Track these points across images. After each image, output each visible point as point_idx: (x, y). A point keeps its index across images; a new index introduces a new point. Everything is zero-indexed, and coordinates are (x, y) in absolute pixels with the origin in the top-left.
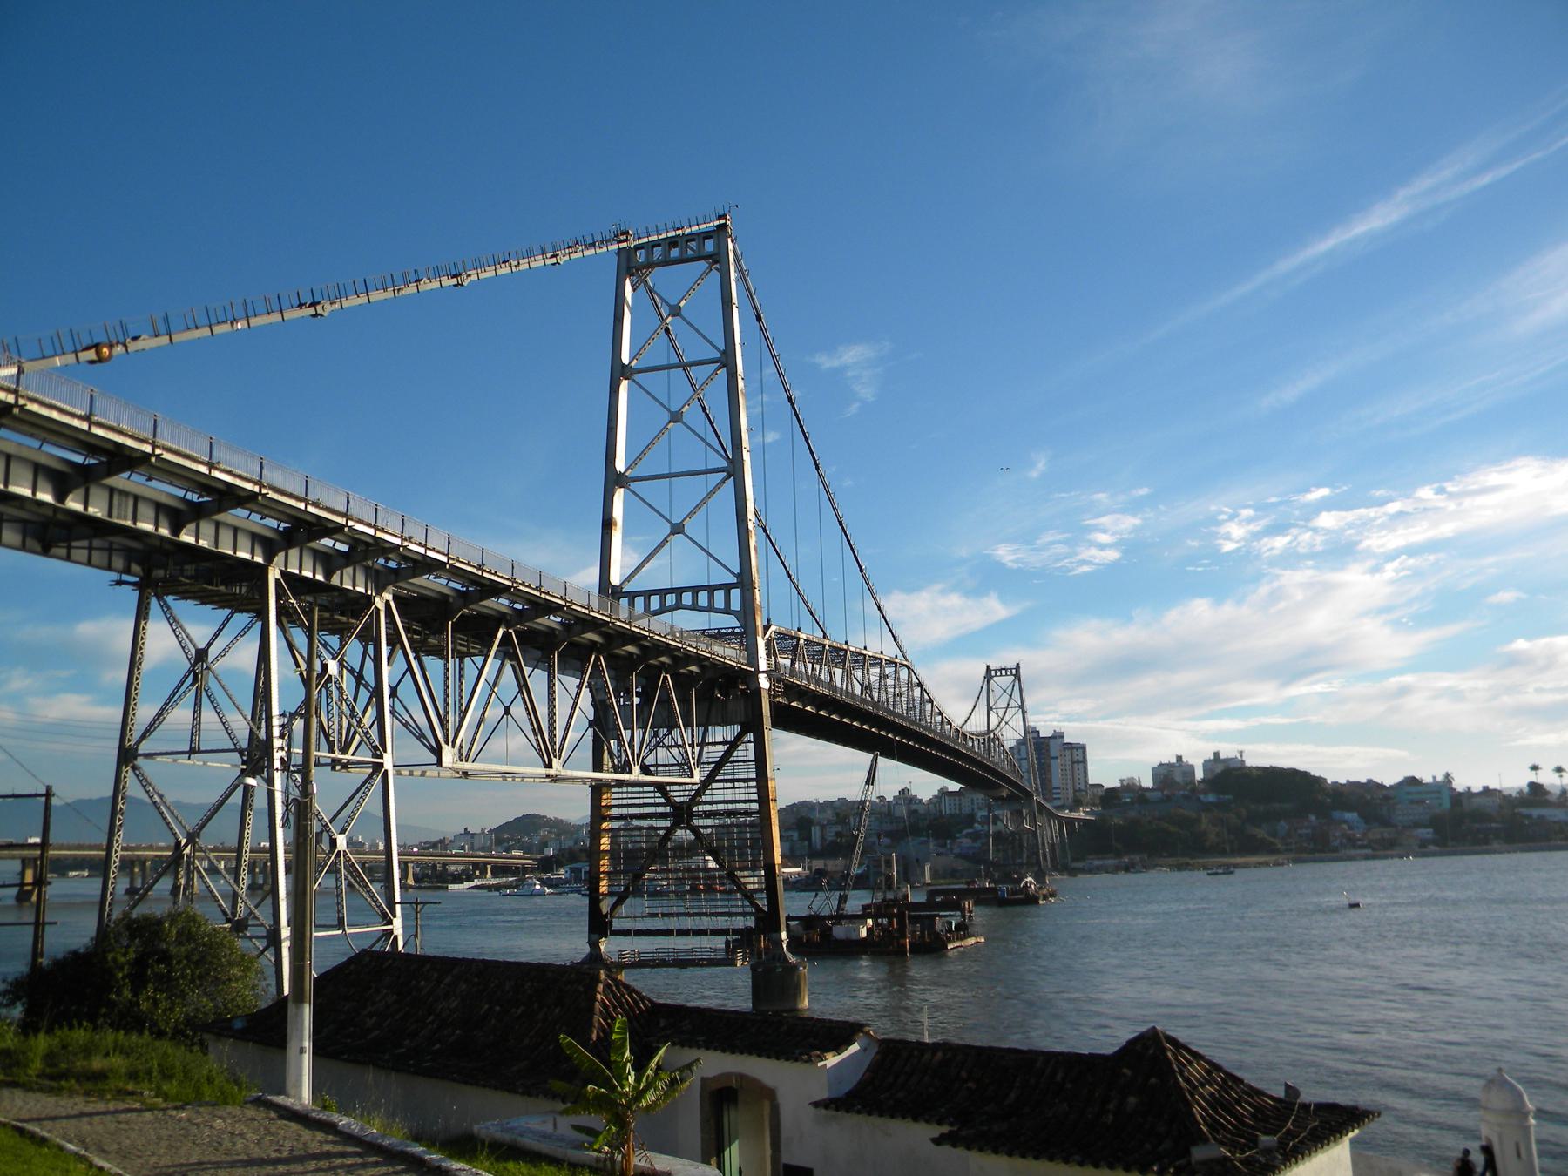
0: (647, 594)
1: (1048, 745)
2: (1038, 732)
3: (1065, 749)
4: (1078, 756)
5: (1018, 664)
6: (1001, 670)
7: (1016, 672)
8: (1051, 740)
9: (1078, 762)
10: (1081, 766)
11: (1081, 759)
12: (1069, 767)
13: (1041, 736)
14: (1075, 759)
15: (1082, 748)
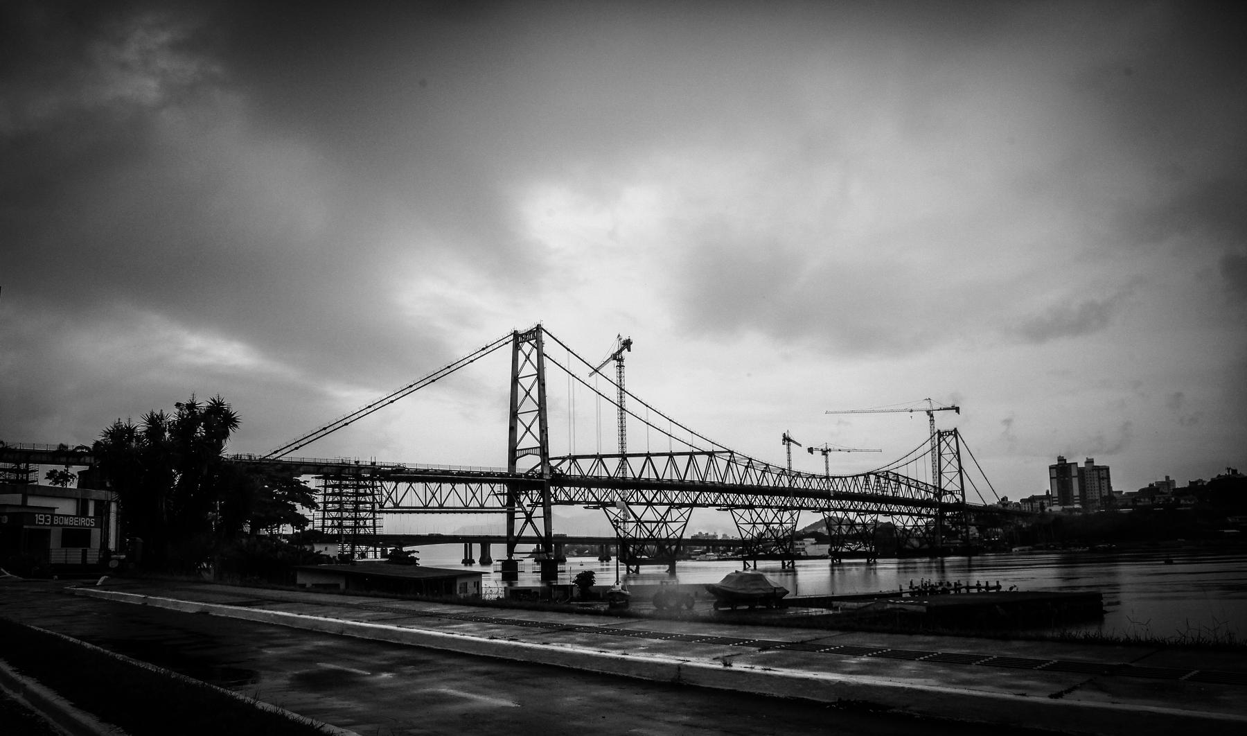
0: (522, 450)
1: (1070, 469)
2: (1065, 460)
3: (1093, 470)
4: (1103, 474)
5: (955, 430)
6: (946, 432)
7: (955, 433)
8: (1072, 465)
9: (1103, 478)
10: (1105, 481)
11: (1105, 476)
12: (1097, 484)
13: (1068, 462)
14: (1101, 476)
15: (1107, 469)
